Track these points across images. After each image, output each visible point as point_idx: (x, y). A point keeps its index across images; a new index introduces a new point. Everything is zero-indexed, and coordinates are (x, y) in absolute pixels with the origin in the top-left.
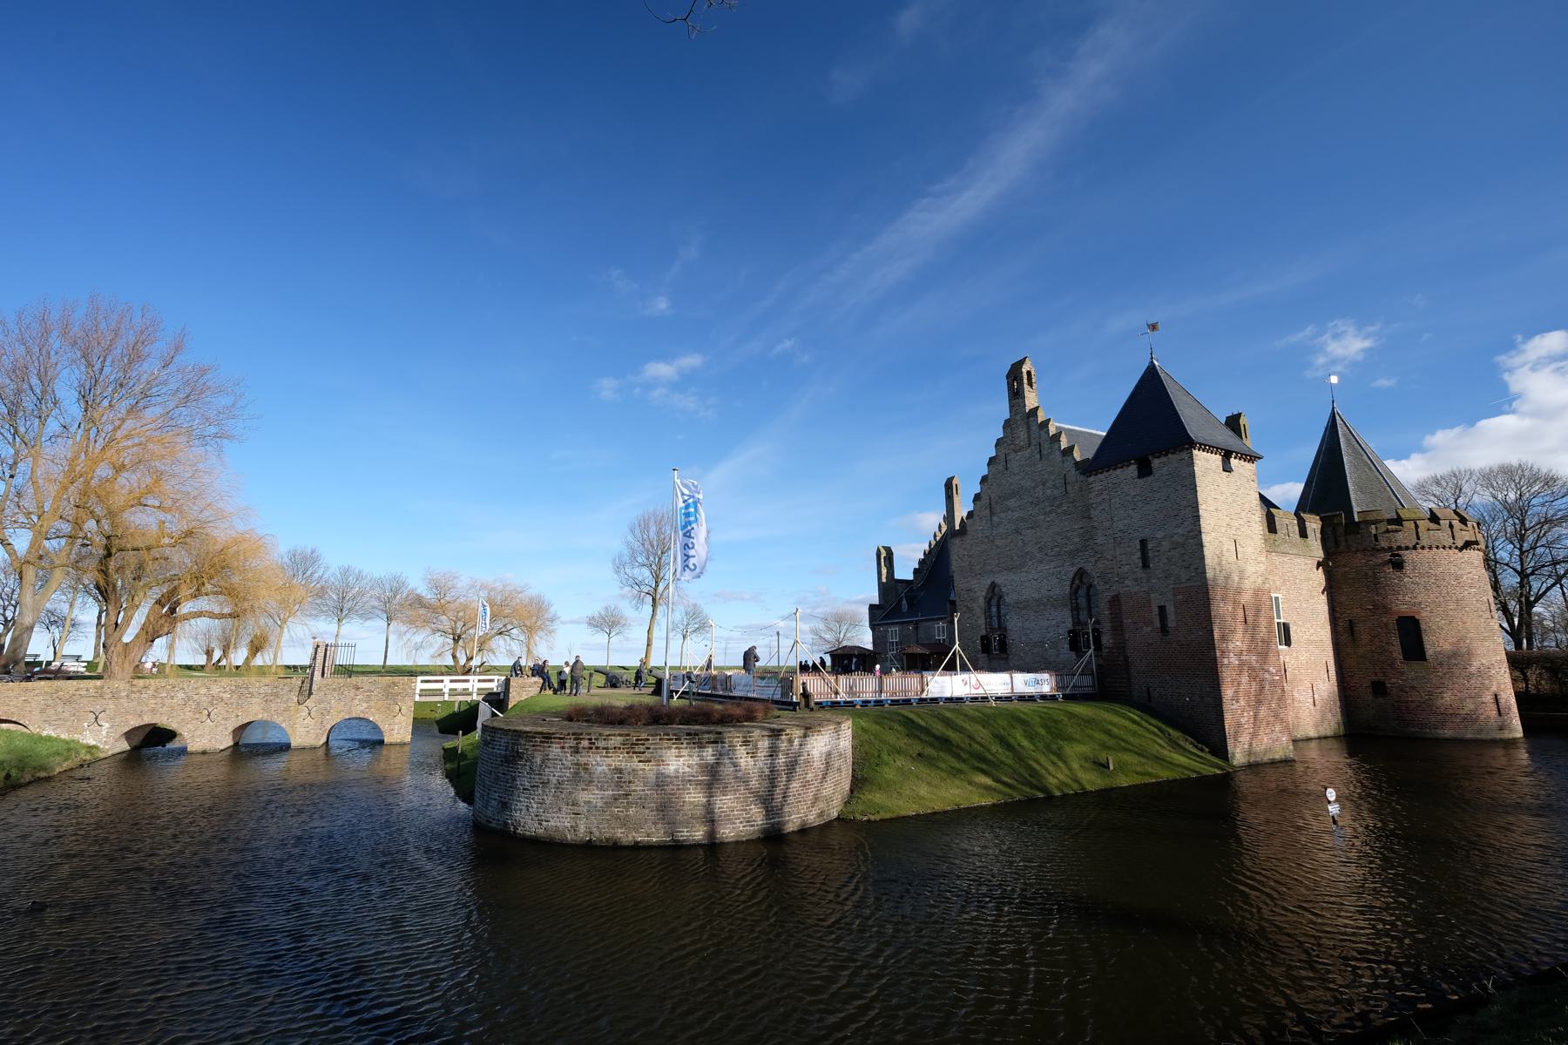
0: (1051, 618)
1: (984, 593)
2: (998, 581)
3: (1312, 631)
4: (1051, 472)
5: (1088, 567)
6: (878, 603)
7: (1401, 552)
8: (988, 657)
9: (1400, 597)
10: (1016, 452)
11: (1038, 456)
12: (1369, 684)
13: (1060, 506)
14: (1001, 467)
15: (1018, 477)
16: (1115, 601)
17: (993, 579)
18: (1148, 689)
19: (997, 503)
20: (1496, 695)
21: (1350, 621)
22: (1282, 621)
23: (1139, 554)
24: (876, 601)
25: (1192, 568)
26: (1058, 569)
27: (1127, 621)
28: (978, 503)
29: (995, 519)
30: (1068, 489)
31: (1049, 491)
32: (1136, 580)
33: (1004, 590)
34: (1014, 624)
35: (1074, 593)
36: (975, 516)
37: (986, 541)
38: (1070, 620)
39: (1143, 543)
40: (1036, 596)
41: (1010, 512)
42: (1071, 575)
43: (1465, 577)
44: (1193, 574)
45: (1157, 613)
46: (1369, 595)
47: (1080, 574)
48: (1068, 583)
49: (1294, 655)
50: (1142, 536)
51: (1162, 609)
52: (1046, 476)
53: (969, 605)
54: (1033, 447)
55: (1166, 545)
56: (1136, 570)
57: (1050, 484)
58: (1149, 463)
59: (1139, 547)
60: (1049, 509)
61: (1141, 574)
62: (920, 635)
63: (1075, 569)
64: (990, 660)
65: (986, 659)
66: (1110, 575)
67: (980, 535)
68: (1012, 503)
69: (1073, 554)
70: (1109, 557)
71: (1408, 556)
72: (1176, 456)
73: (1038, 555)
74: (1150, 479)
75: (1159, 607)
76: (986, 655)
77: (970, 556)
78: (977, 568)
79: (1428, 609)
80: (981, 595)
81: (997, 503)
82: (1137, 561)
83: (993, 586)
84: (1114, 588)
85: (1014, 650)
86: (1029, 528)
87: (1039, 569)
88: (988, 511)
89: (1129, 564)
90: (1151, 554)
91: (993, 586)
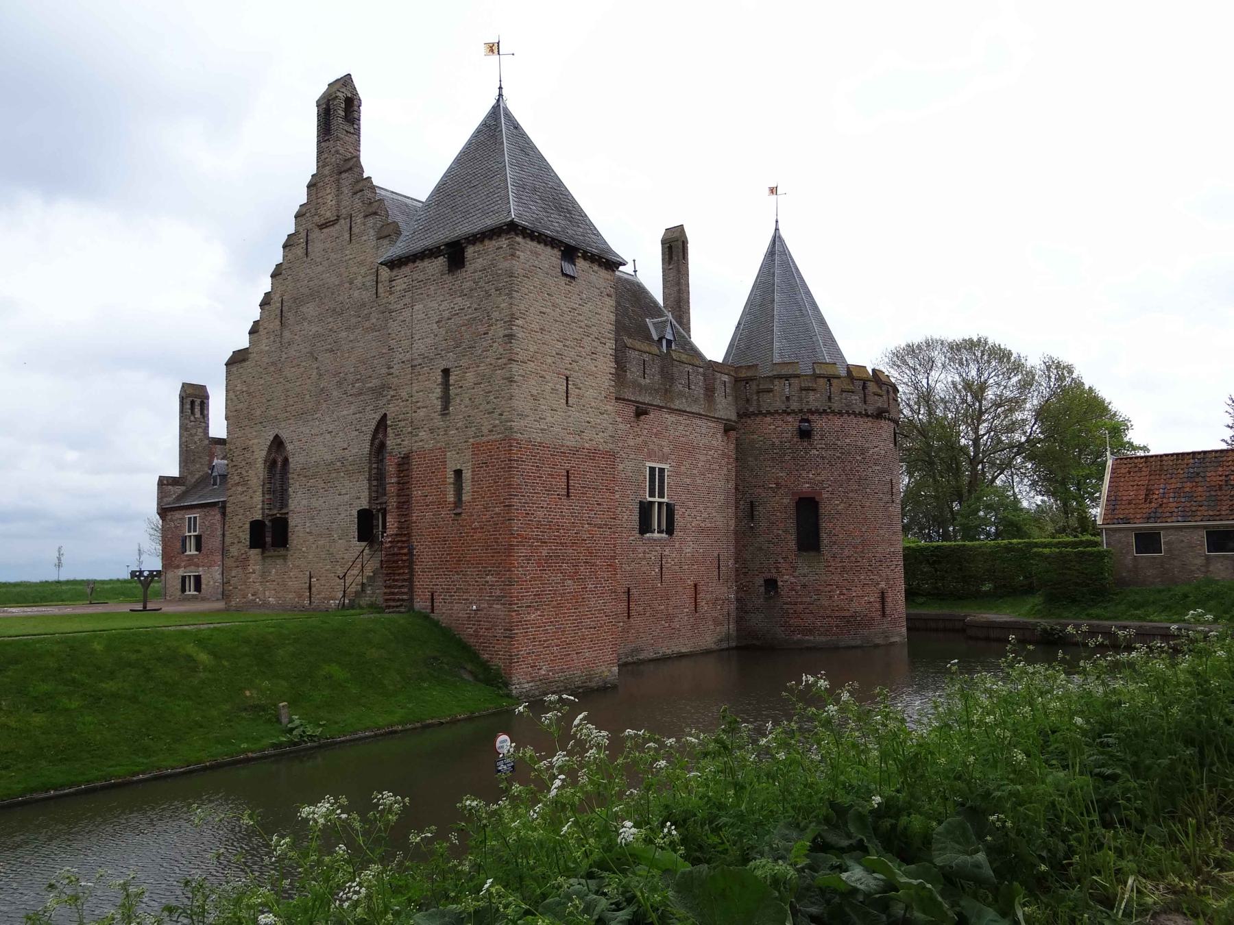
0: (343, 492)
1: (264, 453)
2: (284, 435)
3: (705, 515)
4: (361, 263)
6: (177, 475)
7: (811, 417)
8: (263, 553)
9: (804, 474)
10: (322, 227)
11: (347, 236)
12: (762, 582)
14: (299, 251)
15: (320, 268)
17: (276, 431)
18: (432, 595)
20: (883, 593)
21: (752, 502)
22: (665, 500)
23: (438, 391)
24: (174, 472)
25: (496, 415)
26: (358, 416)
27: (417, 493)
28: (267, 307)
29: (287, 334)
30: (380, 290)
31: (356, 294)
32: (432, 431)
34: (298, 501)
36: (261, 329)
37: (272, 369)
38: (366, 493)
39: (446, 372)
40: (328, 457)
41: (305, 324)
43: (871, 452)
44: (497, 422)
45: (452, 480)
46: (773, 471)
48: (369, 437)
49: (677, 546)
50: (445, 364)
51: (458, 473)
52: (355, 269)
53: (244, 472)
54: (342, 221)
55: (471, 377)
56: (433, 415)
58: (462, 251)
59: (440, 380)
61: (438, 421)
64: (264, 558)
65: (260, 558)
66: (403, 424)
67: (266, 360)
68: (310, 309)
71: (819, 423)
72: (494, 242)
73: (335, 393)
74: (461, 274)
75: (455, 471)
76: (258, 551)
77: (249, 394)
78: (258, 412)
79: (830, 489)
80: (260, 454)
82: (435, 402)
83: (278, 443)
84: (406, 443)
85: (295, 542)
89: (426, 407)
90: (452, 391)
91: (278, 443)
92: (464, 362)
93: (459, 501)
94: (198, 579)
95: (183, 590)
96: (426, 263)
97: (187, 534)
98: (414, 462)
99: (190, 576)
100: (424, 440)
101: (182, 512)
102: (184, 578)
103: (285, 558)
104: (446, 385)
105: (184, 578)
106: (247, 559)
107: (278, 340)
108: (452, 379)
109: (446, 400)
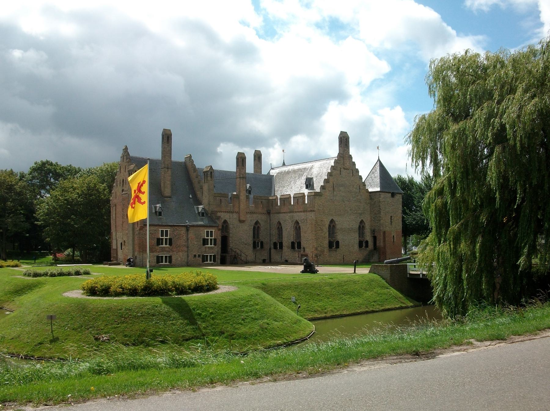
1: (328, 223)
2: (334, 219)
5: (364, 220)
10: (344, 168)
13: (358, 196)
14: (338, 172)
15: (344, 179)
16: (384, 233)
19: (336, 187)
23: (390, 220)
29: (335, 193)
33: (336, 223)
34: (340, 237)
35: (360, 227)
37: (331, 201)
39: (391, 217)
42: (359, 221)
47: (362, 222)
50: (391, 215)
51: (393, 236)
57: (355, 186)
60: (354, 196)
62: (189, 236)
63: (360, 220)
64: (329, 251)
68: (341, 188)
69: (361, 214)
70: (384, 219)
78: (326, 211)
81: (336, 187)
83: (332, 221)
86: (347, 201)
87: (350, 217)
88: (332, 189)
90: (392, 220)
91: (332, 221)
92: (394, 215)
93: (394, 241)
94: (170, 257)
95: (158, 262)
96: (387, 194)
97: (160, 237)
98: (386, 233)
99: (162, 257)
100: (387, 229)
101: (157, 227)
102: (158, 257)
103: (336, 251)
104: (391, 219)
105: (158, 257)
106: (324, 251)
107: (332, 194)
108: (392, 218)
109: (391, 222)
